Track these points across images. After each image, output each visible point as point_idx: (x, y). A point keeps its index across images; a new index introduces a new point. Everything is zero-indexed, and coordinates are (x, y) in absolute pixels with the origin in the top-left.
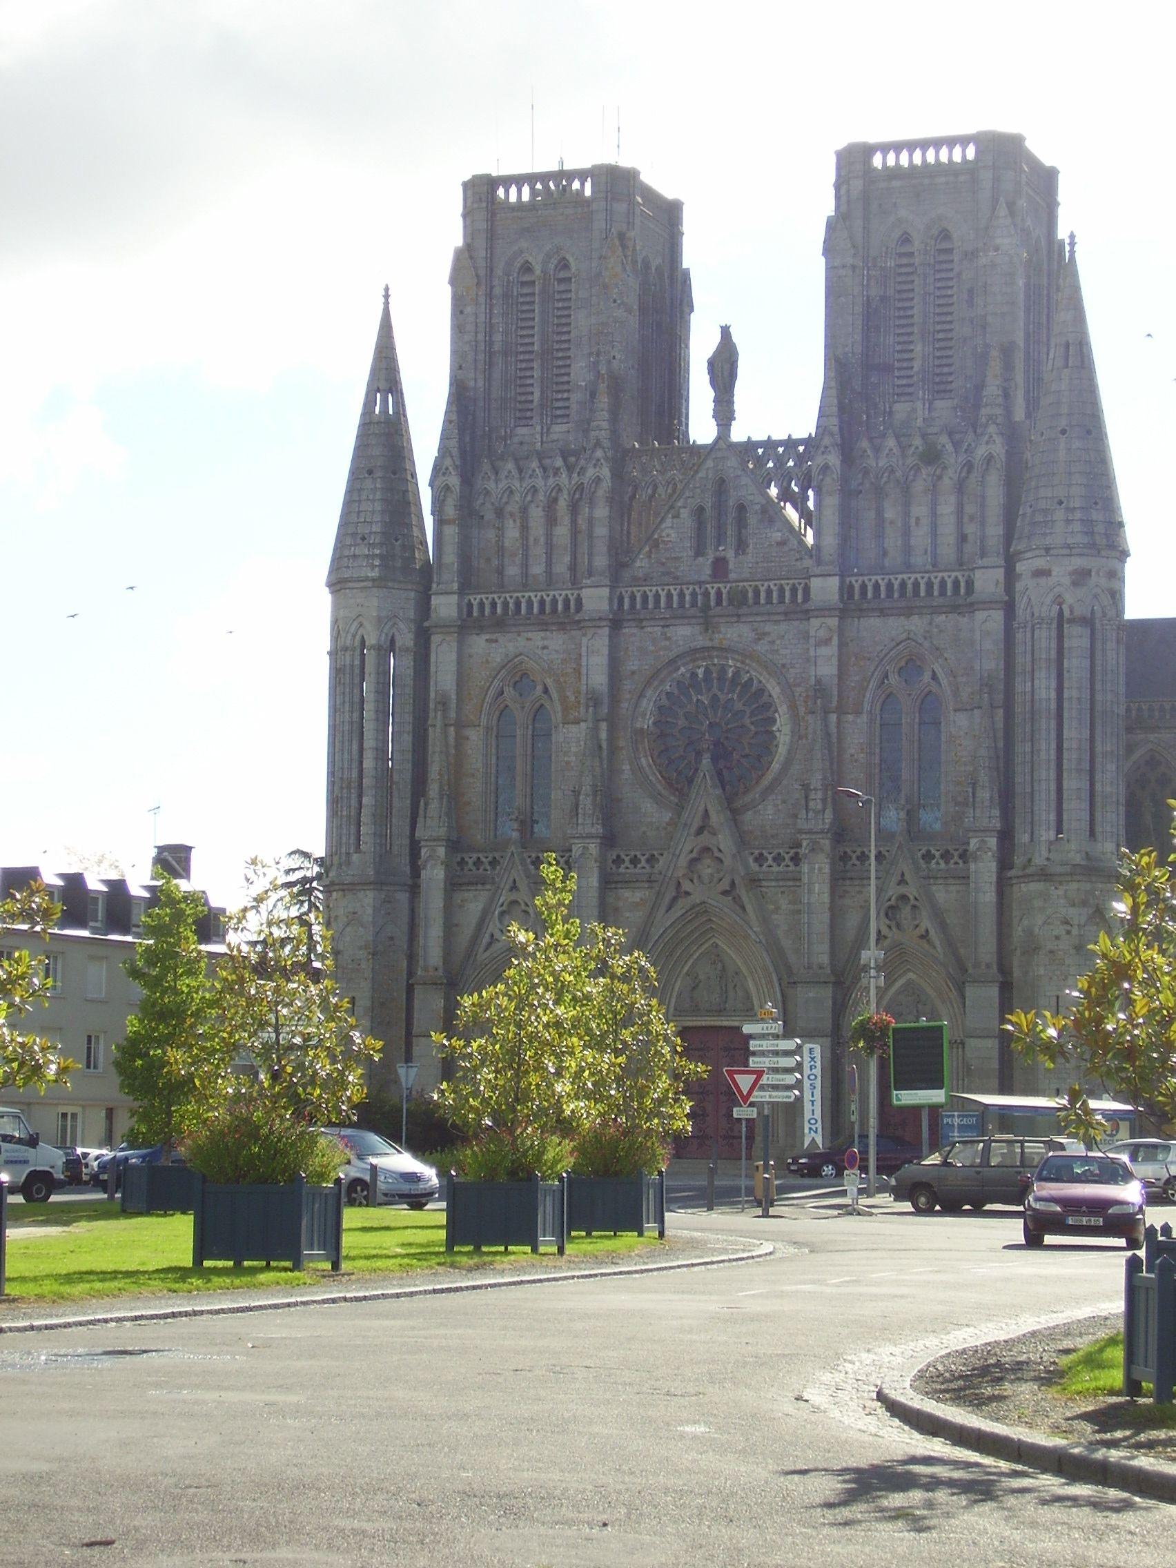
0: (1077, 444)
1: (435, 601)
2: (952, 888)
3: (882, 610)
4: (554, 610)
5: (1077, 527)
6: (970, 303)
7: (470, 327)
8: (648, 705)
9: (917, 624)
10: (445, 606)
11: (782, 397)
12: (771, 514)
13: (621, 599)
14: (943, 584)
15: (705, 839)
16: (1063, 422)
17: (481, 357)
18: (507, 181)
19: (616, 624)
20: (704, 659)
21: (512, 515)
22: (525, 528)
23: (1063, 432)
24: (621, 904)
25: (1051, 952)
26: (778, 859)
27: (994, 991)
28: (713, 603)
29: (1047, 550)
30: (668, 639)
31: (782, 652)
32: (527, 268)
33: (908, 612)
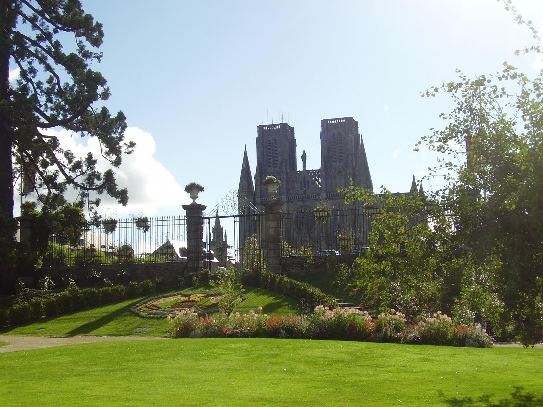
11: (314, 163)
12: (313, 183)
18: (265, 126)
19: (288, 202)
32: (269, 141)
33: (337, 199)
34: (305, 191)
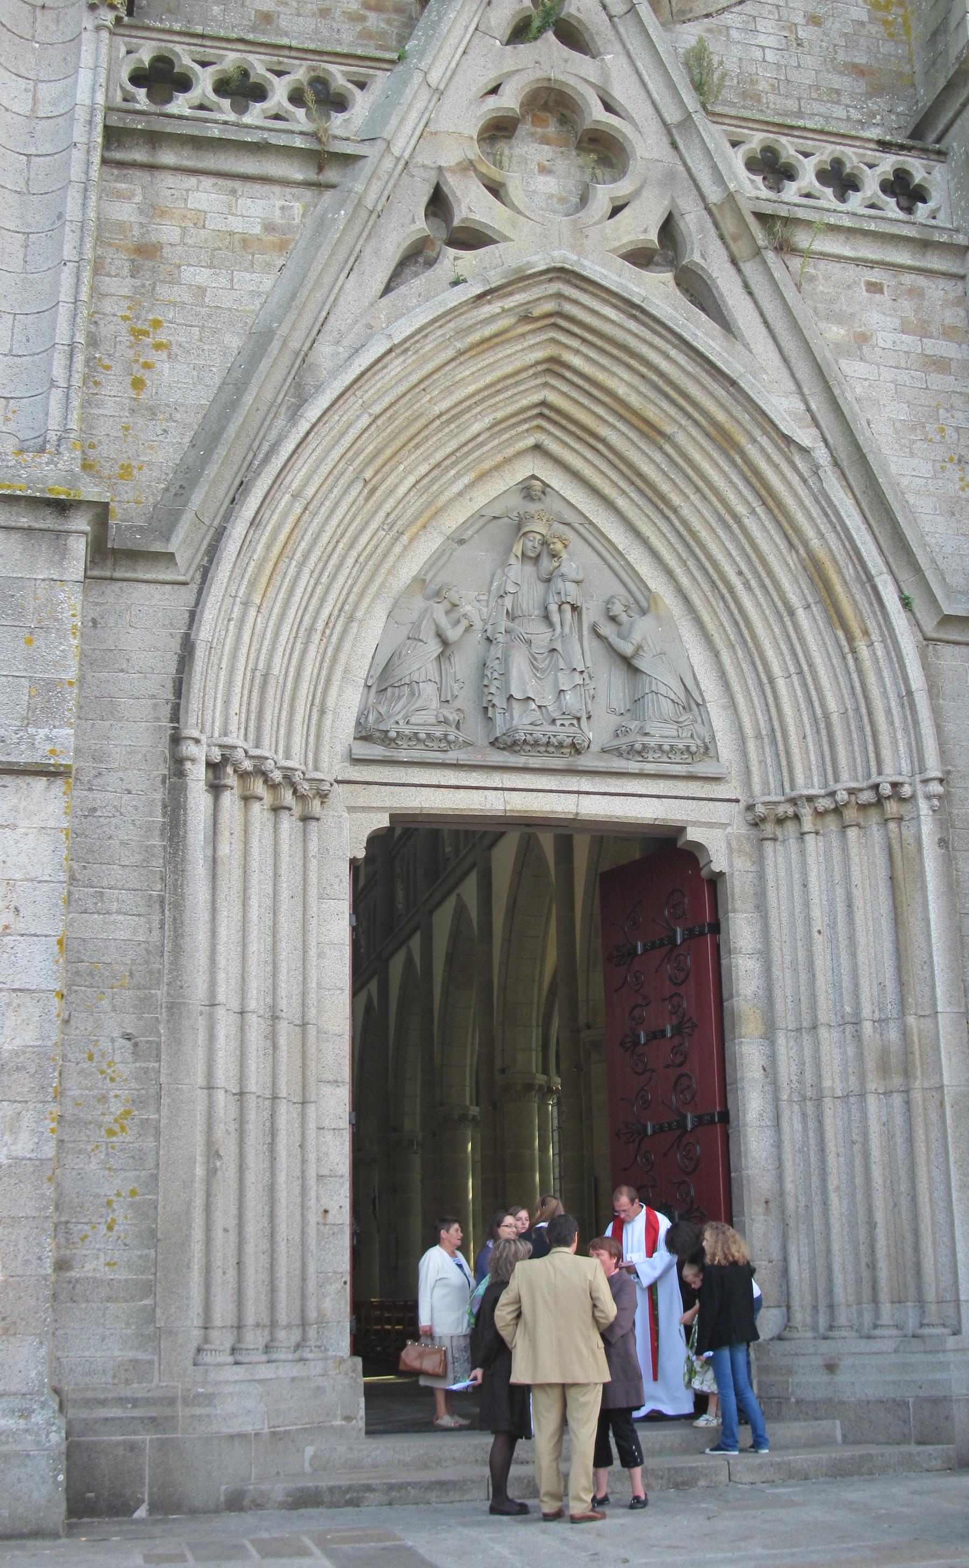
15: (548, 59)
24: (168, 232)
26: (840, 180)
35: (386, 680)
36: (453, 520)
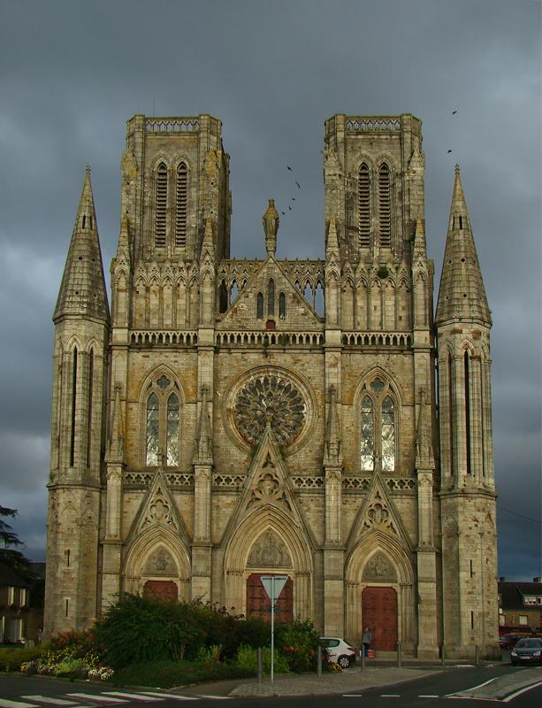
0: (471, 267)
1: (115, 332)
2: (404, 501)
3: (362, 351)
4: (181, 343)
5: (476, 308)
6: (401, 199)
7: (133, 192)
8: (233, 395)
9: (382, 359)
10: (120, 335)
13: (219, 337)
14: (395, 338)
15: (269, 469)
16: (463, 256)
17: (138, 208)
19: (217, 350)
20: (264, 372)
21: (154, 292)
22: (161, 299)
23: (463, 260)
24: (220, 504)
25: (467, 536)
27: (433, 557)
28: (270, 342)
29: (460, 319)
30: (245, 360)
31: (309, 370)
32: (162, 166)
33: (377, 352)
34: (271, 324)
35: (250, 556)
36: (259, 535)
